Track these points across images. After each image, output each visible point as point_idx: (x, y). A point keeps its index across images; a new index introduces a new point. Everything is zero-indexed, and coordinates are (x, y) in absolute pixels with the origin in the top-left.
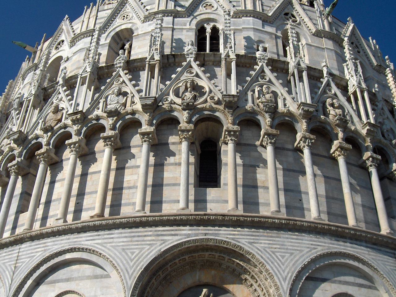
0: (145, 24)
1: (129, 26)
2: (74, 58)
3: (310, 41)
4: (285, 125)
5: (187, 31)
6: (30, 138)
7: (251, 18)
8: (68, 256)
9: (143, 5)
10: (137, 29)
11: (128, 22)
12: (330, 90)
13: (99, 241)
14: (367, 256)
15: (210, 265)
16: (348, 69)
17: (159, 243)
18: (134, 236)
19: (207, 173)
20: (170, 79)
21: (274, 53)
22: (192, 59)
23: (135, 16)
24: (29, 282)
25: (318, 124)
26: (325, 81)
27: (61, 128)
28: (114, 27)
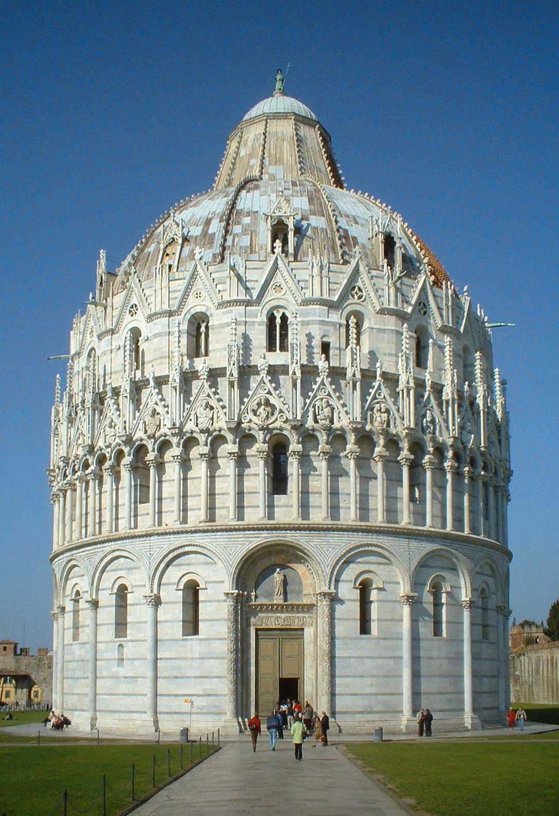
0: (219, 310)
1: (203, 309)
2: (155, 341)
3: (373, 323)
4: (338, 438)
5: (259, 325)
6: (134, 439)
7: (318, 306)
8: (187, 549)
9: (215, 283)
10: (212, 315)
11: (202, 303)
12: (379, 394)
13: (208, 540)
14: (386, 544)
15: (280, 552)
16: (402, 361)
17: (248, 543)
18: (231, 538)
19: (278, 483)
20: (247, 396)
21: (336, 349)
22: (265, 375)
23: (208, 296)
24: (162, 565)
25: (365, 433)
26: (376, 384)
27: (161, 436)
28: (188, 308)
